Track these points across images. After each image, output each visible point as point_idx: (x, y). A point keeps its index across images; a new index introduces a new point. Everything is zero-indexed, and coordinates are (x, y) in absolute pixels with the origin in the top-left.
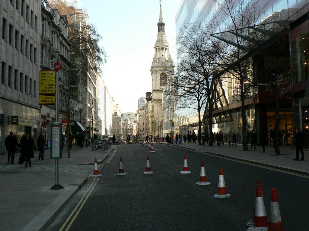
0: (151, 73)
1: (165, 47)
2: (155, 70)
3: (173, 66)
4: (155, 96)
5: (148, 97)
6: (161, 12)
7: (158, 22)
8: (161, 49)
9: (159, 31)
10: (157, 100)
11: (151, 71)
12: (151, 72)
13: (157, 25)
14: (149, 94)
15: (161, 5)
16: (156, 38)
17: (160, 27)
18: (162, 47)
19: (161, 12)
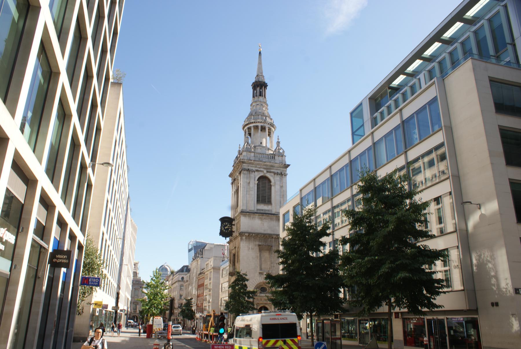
0: (230, 180)
1: (267, 126)
2: (247, 168)
3: (285, 164)
4: (245, 224)
5: (224, 229)
6: (260, 63)
7: (254, 81)
8: (260, 127)
9: (254, 97)
10: (249, 233)
11: (230, 175)
12: (230, 179)
13: (251, 87)
14: (225, 221)
15: (260, 53)
16: (246, 111)
17: (258, 89)
18: (262, 124)
19: (260, 63)
